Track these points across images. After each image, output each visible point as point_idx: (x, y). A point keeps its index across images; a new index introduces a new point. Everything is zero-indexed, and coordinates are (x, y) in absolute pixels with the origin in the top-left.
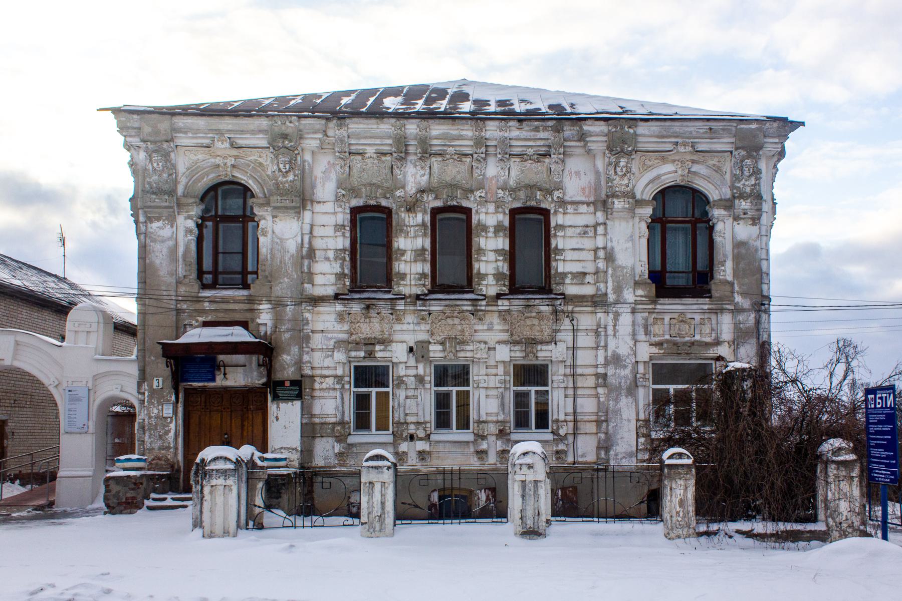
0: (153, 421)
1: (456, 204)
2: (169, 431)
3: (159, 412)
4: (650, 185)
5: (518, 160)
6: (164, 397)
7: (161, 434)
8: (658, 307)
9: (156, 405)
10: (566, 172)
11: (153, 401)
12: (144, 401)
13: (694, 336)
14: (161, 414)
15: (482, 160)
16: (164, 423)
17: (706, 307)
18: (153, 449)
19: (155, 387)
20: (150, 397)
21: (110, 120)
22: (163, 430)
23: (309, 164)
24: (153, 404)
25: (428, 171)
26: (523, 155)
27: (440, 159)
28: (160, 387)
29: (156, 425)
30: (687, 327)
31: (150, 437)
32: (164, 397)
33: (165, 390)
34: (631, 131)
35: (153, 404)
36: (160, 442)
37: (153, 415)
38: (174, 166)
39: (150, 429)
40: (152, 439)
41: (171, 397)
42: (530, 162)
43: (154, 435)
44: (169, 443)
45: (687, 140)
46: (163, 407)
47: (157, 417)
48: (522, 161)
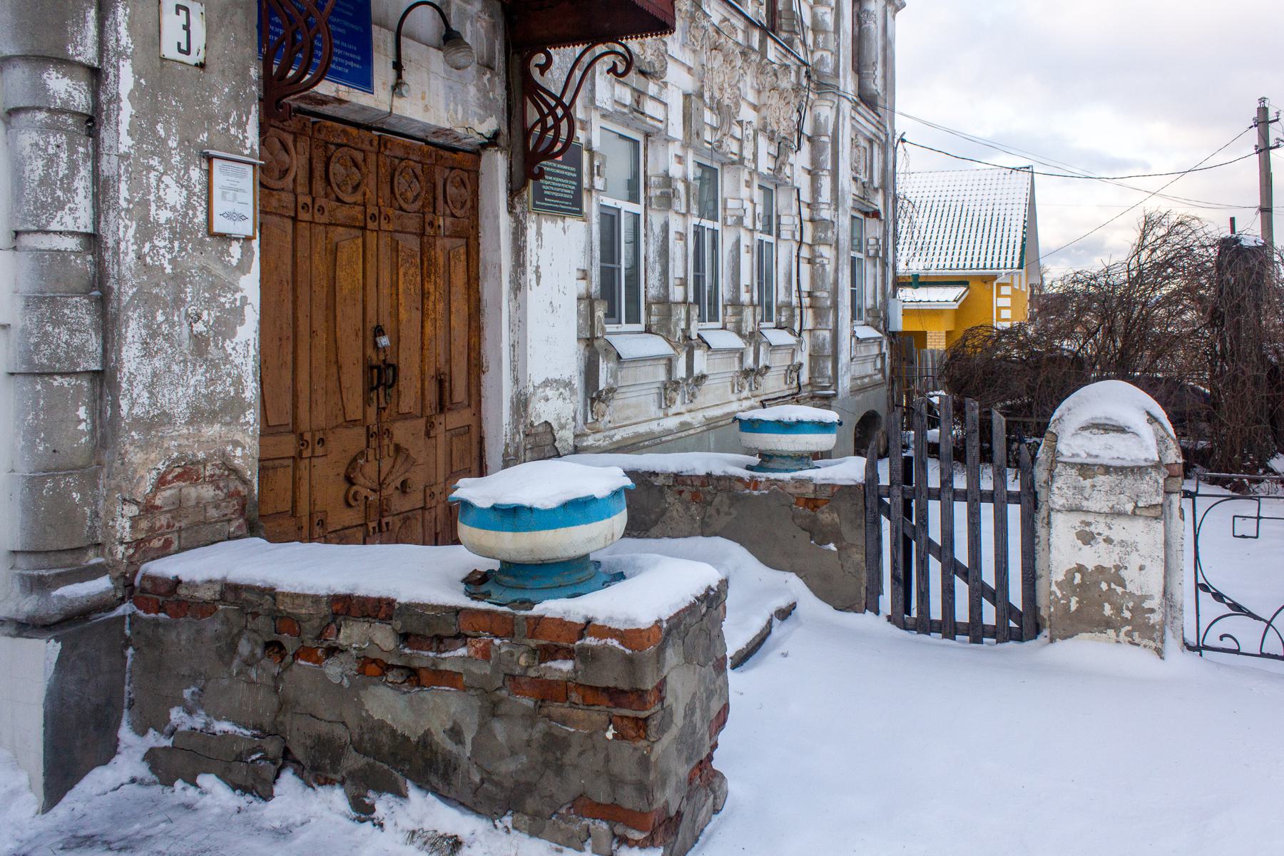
0: (163, 253)
2: (237, 314)
3: (188, 205)
6: (211, 118)
7: (199, 327)
9: (176, 159)
11: (160, 128)
12: (92, 123)
14: (201, 217)
16: (217, 269)
18: (165, 418)
19: (169, 50)
20: (149, 110)
22: (209, 303)
24: (160, 149)
28: (193, 59)
29: (179, 278)
31: (148, 352)
32: (211, 118)
33: (214, 77)
35: (160, 149)
36: (197, 377)
37: (164, 215)
39: (148, 301)
40: (158, 363)
41: (241, 125)
43: (168, 338)
44: (238, 382)
46: (209, 173)
47: (180, 231)
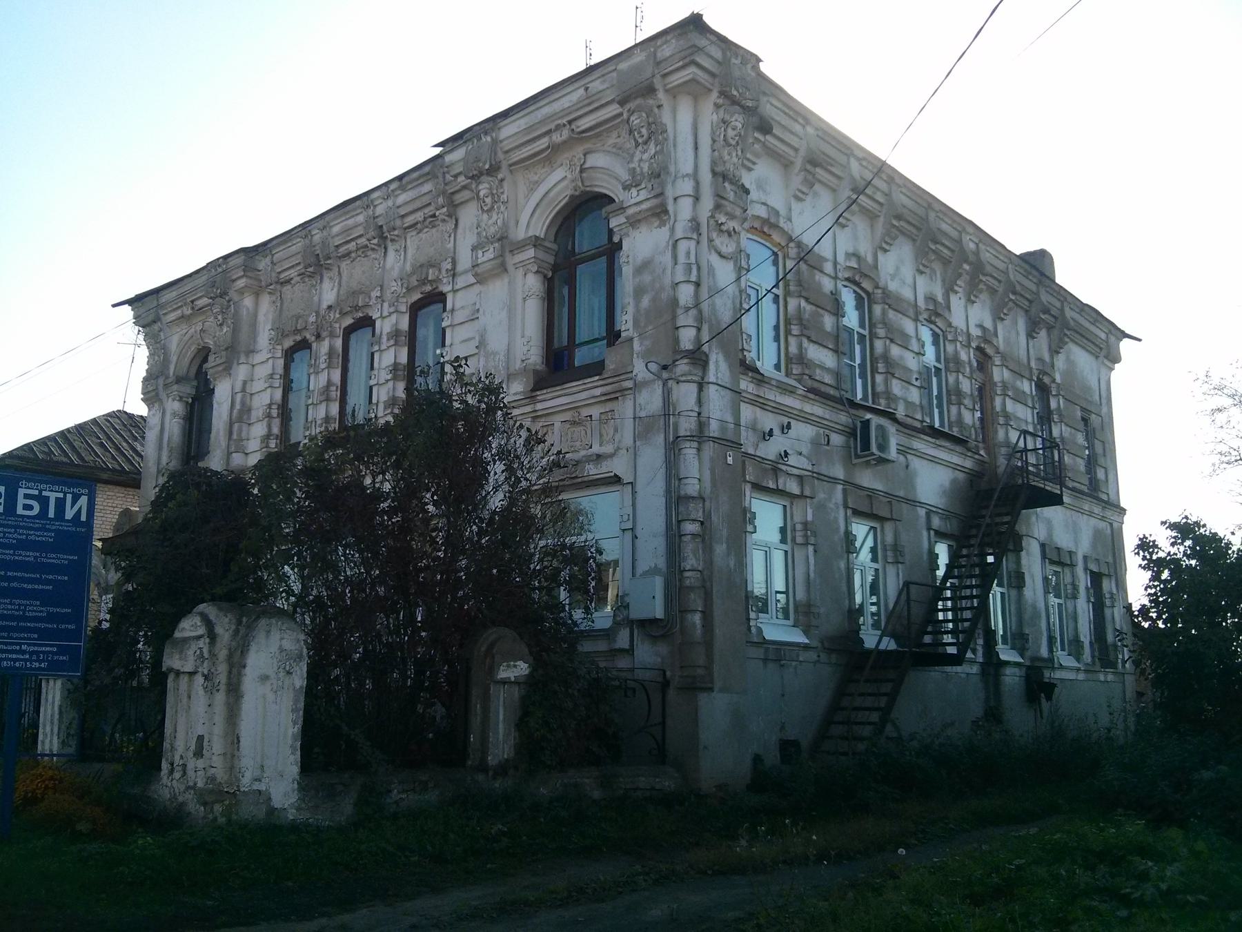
1: (361, 315)
4: (538, 212)
5: (414, 233)
8: (539, 406)
10: (460, 231)
13: (591, 448)
15: (376, 247)
17: (598, 392)
21: (127, 311)
23: (248, 309)
25: (337, 281)
26: (417, 223)
27: (349, 262)
30: (583, 432)
34: (489, 139)
38: (164, 348)
42: (426, 230)
45: (559, 122)
48: (418, 233)
